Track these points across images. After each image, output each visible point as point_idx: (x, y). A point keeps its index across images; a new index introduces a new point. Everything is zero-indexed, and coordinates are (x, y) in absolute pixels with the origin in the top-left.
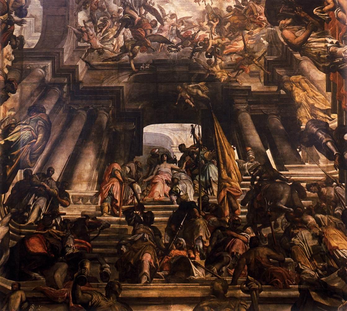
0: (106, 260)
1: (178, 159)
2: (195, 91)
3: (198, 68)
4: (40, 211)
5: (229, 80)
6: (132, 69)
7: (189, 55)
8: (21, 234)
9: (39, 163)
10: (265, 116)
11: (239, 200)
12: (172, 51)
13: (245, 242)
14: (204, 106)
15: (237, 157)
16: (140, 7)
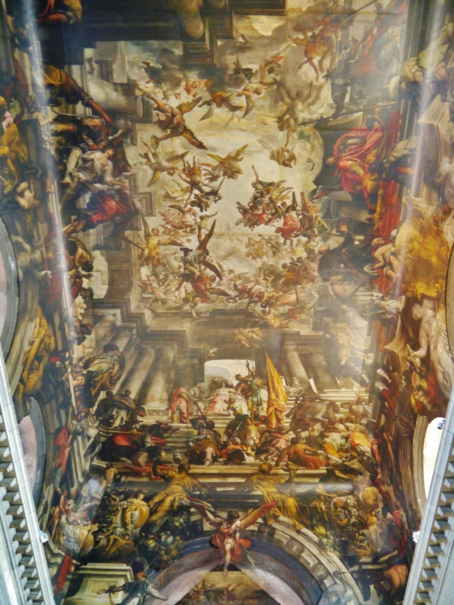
0: (178, 450)
1: (235, 385)
2: (250, 334)
3: (255, 317)
4: (122, 419)
5: (281, 327)
6: (192, 317)
7: (245, 306)
8: (109, 433)
9: (118, 386)
10: (311, 354)
11: (284, 413)
12: (230, 302)
13: (287, 441)
14: (258, 346)
15: (284, 384)
16: (199, 263)
